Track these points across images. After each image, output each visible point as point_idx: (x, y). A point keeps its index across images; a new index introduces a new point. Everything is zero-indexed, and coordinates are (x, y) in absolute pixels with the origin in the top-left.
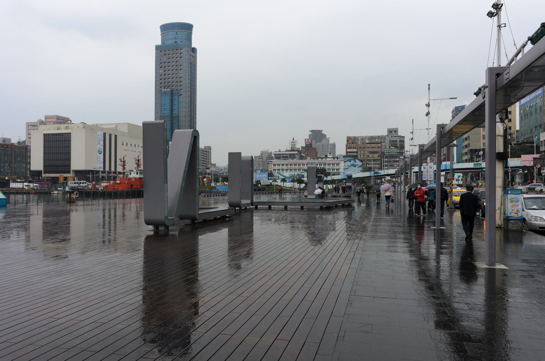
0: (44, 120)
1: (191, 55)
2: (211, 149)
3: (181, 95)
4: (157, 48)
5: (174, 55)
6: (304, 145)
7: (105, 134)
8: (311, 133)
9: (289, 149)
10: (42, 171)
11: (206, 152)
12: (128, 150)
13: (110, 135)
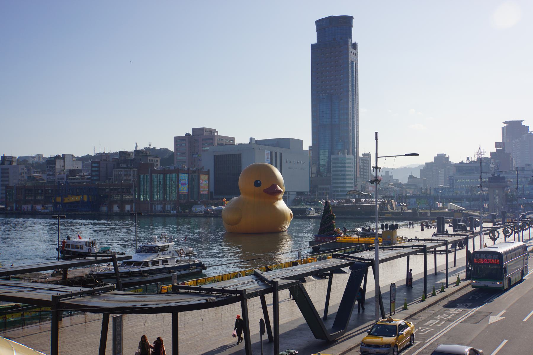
0: (191, 133)
1: (352, 52)
2: (370, 156)
3: (342, 99)
4: (313, 46)
5: (332, 54)
6: (494, 150)
7: (271, 153)
8: (505, 125)
9: (474, 158)
10: (213, 193)
11: (365, 160)
12: (292, 168)
13: (276, 153)
